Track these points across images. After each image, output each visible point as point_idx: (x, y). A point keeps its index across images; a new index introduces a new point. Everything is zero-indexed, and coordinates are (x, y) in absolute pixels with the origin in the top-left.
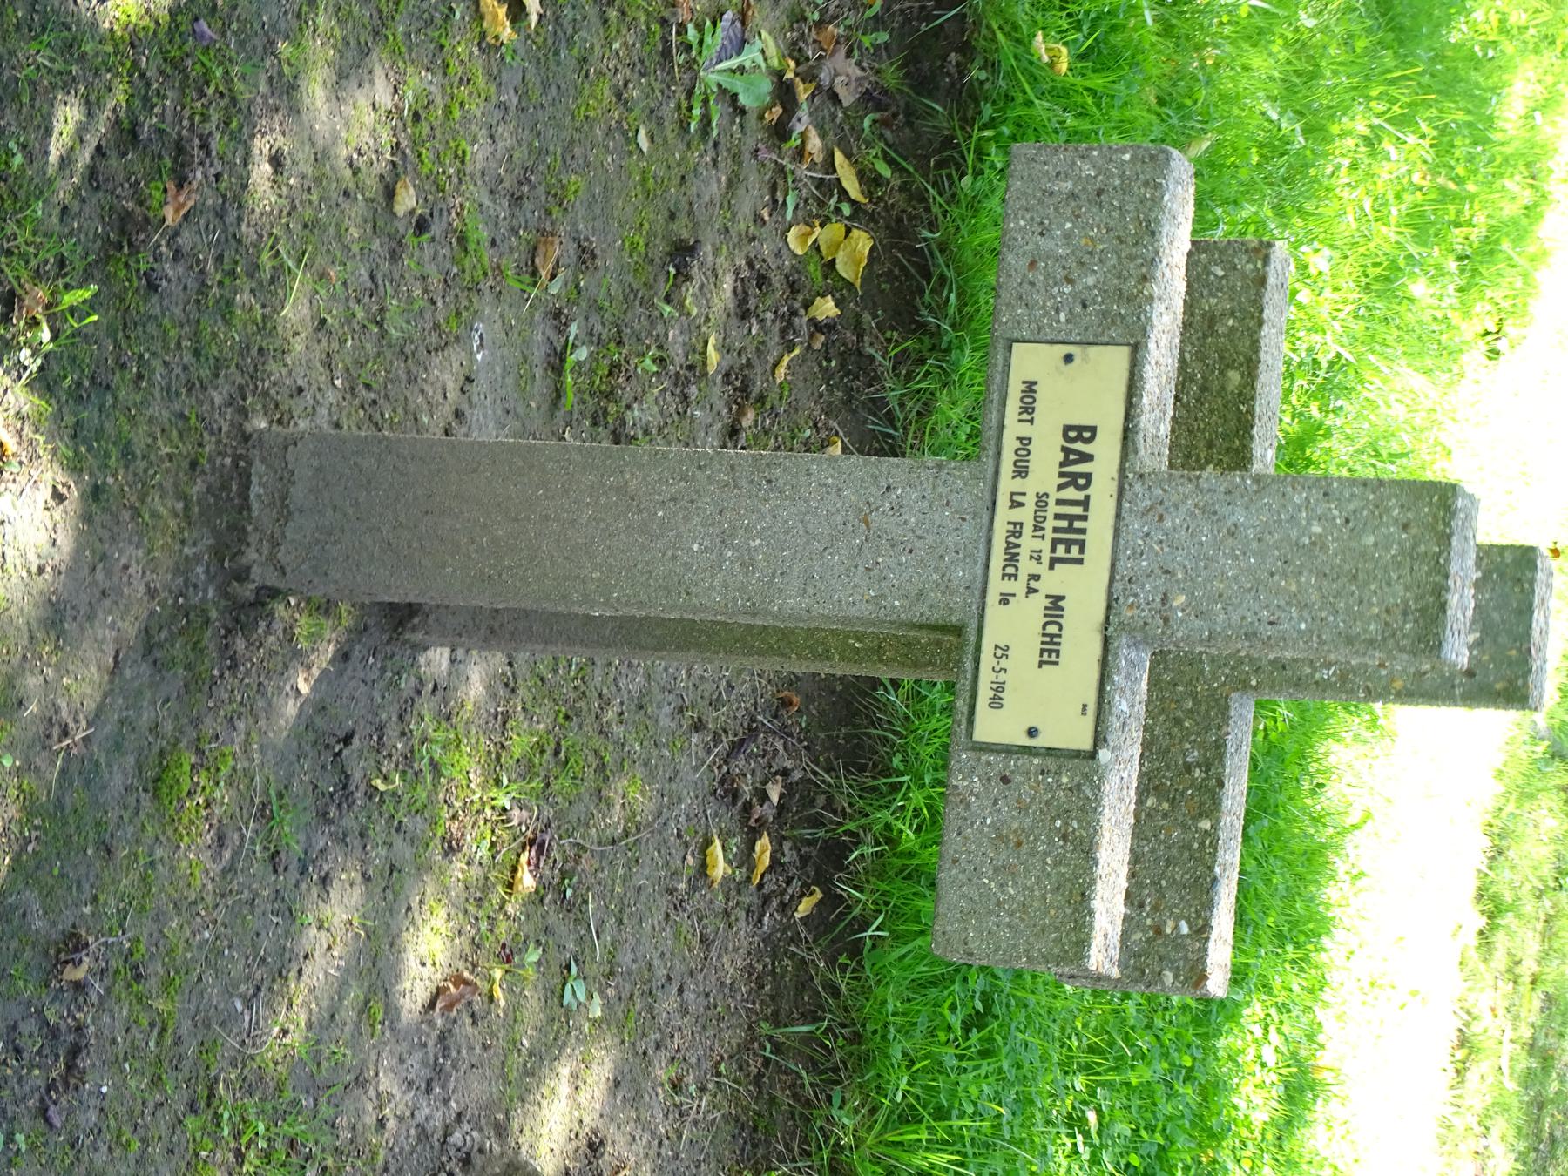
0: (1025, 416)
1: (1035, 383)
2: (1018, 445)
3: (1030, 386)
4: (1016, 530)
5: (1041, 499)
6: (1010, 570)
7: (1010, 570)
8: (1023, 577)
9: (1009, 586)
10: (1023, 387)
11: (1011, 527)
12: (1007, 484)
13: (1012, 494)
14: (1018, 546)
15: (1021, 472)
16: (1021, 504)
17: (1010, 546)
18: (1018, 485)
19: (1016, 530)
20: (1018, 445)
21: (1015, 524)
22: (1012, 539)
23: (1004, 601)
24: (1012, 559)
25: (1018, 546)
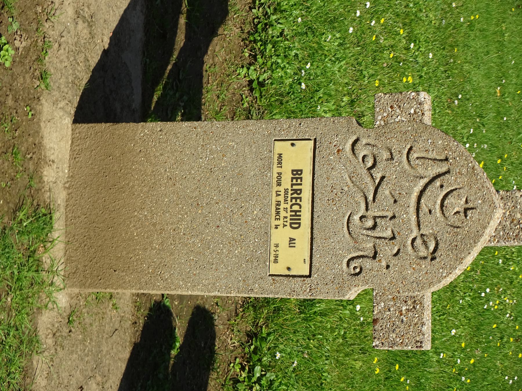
0: (279, 165)
1: (282, 154)
2: (277, 175)
4: (278, 204)
5: (286, 190)
6: (278, 217)
7: (278, 217)
8: (282, 218)
9: (277, 222)
12: (275, 188)
13: (277, 192)
14: (280, 209)
15: (279, 184)
16: (280, 195)
17: (277, 209)
19: (278, 204)
20: (277, 175)
21: (278, 202)
22: (277, 207)
23: (276, 228)
24: (278, 213)
25: (280, 209)
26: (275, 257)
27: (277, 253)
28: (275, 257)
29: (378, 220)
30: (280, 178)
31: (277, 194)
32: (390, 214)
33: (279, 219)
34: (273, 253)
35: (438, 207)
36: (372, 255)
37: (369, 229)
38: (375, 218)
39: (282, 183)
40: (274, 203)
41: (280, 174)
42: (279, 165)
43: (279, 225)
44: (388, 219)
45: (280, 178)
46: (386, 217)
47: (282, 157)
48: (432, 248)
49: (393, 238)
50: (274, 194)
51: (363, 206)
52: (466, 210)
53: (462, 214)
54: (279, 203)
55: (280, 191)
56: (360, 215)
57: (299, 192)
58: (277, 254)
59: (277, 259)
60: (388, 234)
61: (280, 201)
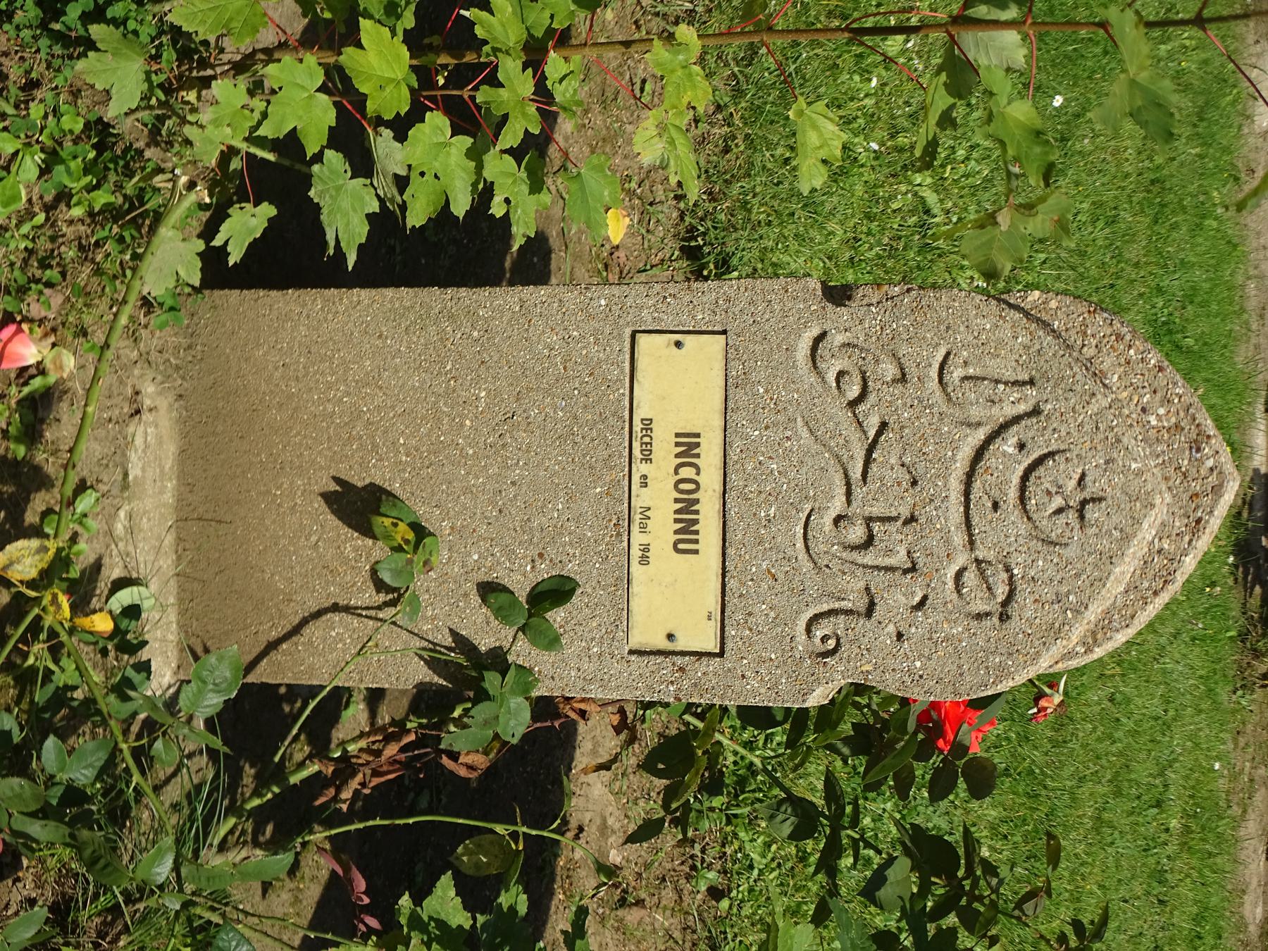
28: (643, 550)
29: (876, 527)
32: (905, 512)
35: (1013, 493)
36: (863, 610)
37: (854, 548)
38: (869, 520)
44: (899, 523)
46: (895, 519)
48: (1001, 591)
49: (913, 569)
51: (840, 491)
52: (1084, 503)
53: (1072, 516)
56: (833, 514)
60: (899, 558)
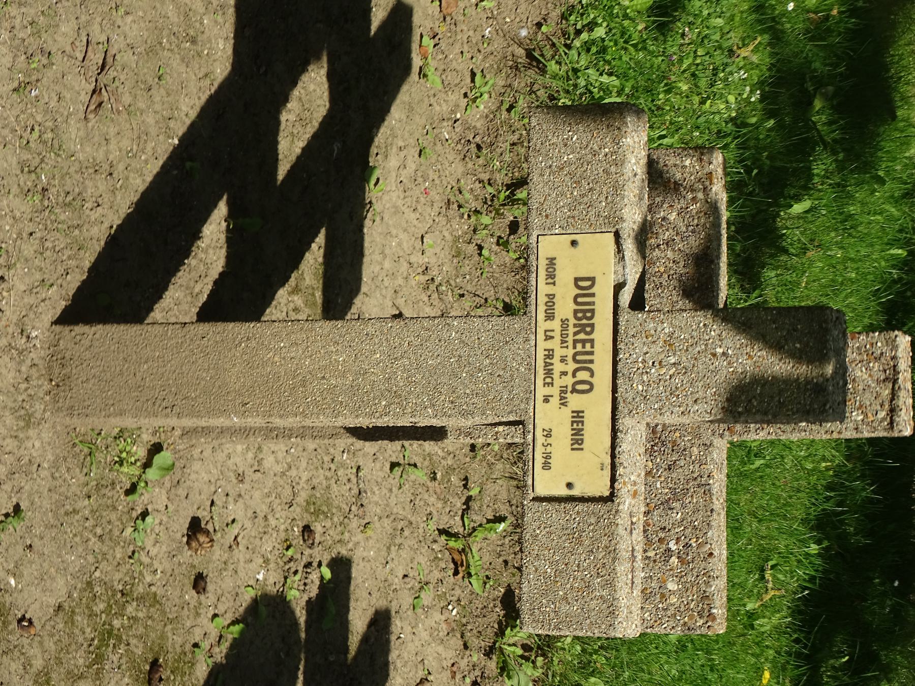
0: (550, 281)
1: (555, 259)
2: (548, 300)
3: (552, 261)
4: (550, 354)
9: (548, 391)
10: (547, 262)
11: (546, 353)
12: (543, 325)
13: (546, 331)
14: (552, 364)
15: (550, 317)
16: (552, 337)
17: (547, 364)
18: (549, 325)
19: (550, 354)
21: (549, 350)
22: (548, 360)
23: (546, 400)
24: (549, 373)
25: (552, 364)
26: (546, 458)
27: (549, 449)
28: (546, 458)
30: (551, 304)
31: (546, 336)
33: (552, 384)
34: (539, 450)
39: (556, 315)
40: (541, 354)
41: (551, 297)
42: (552, 281)
43: (552, 396)
45: (551, 304)
47: (555, 264)
50: (541, 336)
54: (551, 352)
55: (553, 331)
57: (588, 329)
58: (548, 451)
59: (549, 461)
61: (553, 350)
